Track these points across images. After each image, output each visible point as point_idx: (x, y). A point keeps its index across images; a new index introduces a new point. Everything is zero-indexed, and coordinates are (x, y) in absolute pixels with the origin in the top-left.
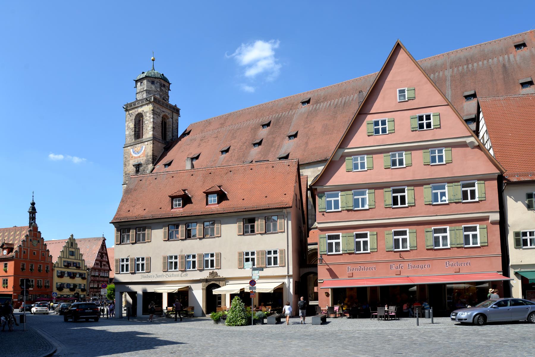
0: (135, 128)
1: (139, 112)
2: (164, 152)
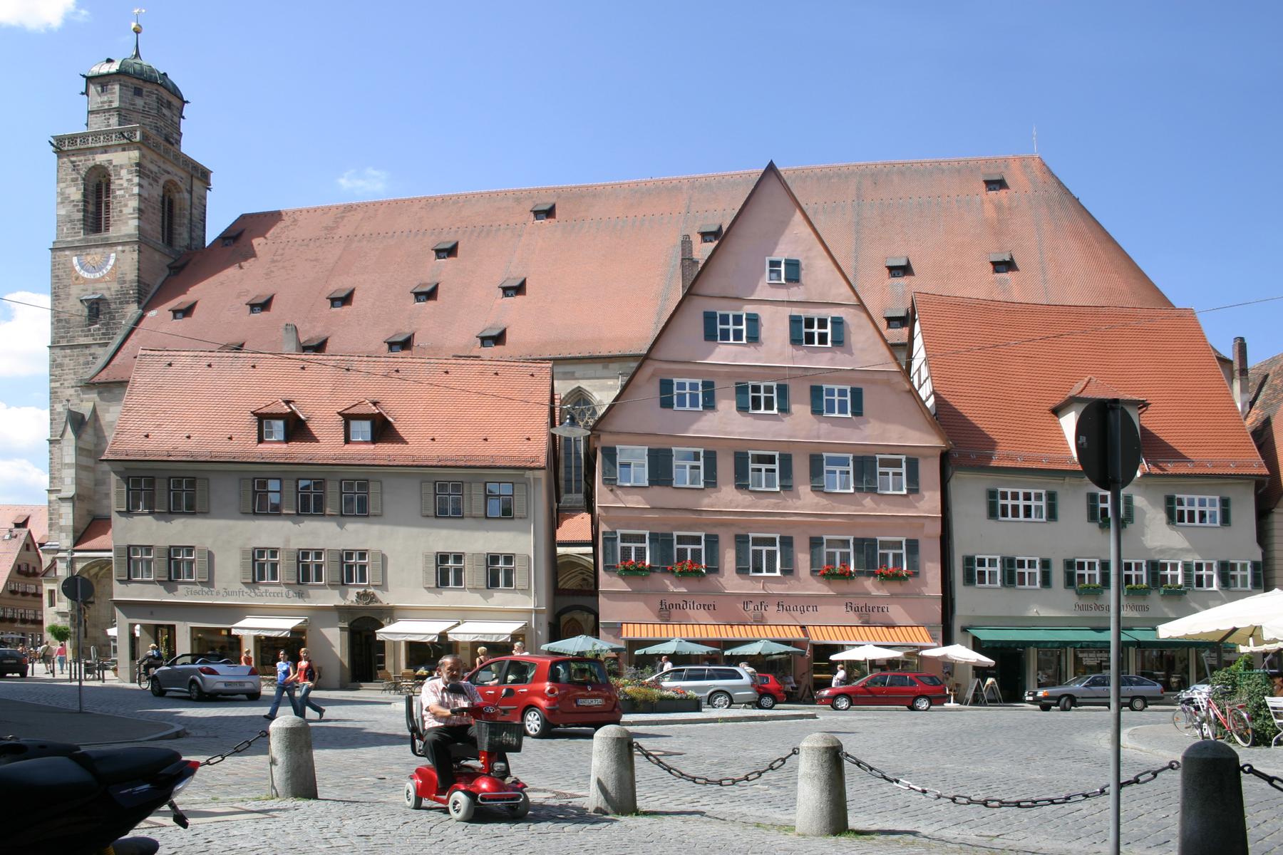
0: (85, 201)
1: (98, 163)
2: (168, 276)
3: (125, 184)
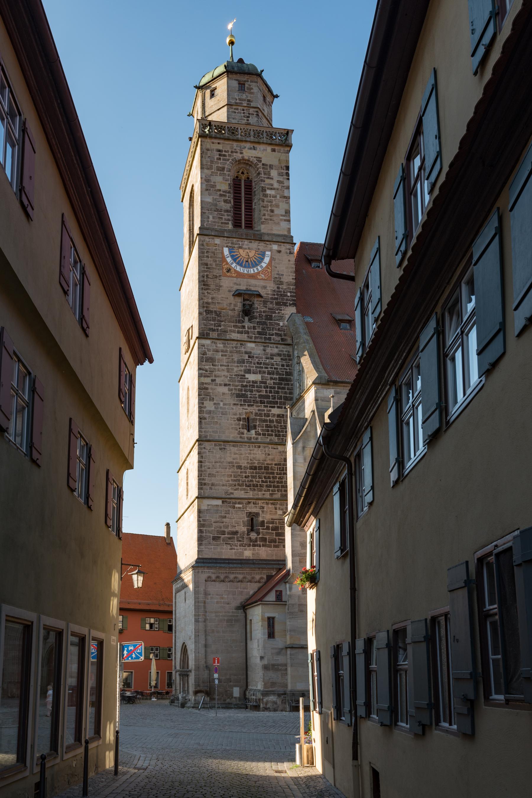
1: (246, 158)
3: (276, 185)
